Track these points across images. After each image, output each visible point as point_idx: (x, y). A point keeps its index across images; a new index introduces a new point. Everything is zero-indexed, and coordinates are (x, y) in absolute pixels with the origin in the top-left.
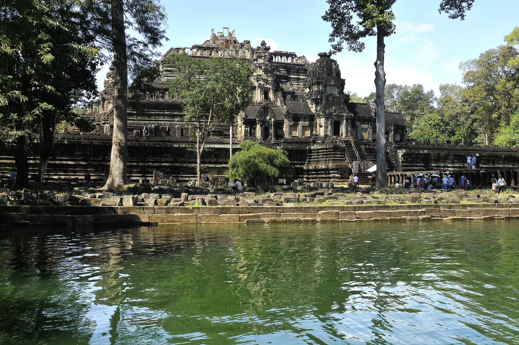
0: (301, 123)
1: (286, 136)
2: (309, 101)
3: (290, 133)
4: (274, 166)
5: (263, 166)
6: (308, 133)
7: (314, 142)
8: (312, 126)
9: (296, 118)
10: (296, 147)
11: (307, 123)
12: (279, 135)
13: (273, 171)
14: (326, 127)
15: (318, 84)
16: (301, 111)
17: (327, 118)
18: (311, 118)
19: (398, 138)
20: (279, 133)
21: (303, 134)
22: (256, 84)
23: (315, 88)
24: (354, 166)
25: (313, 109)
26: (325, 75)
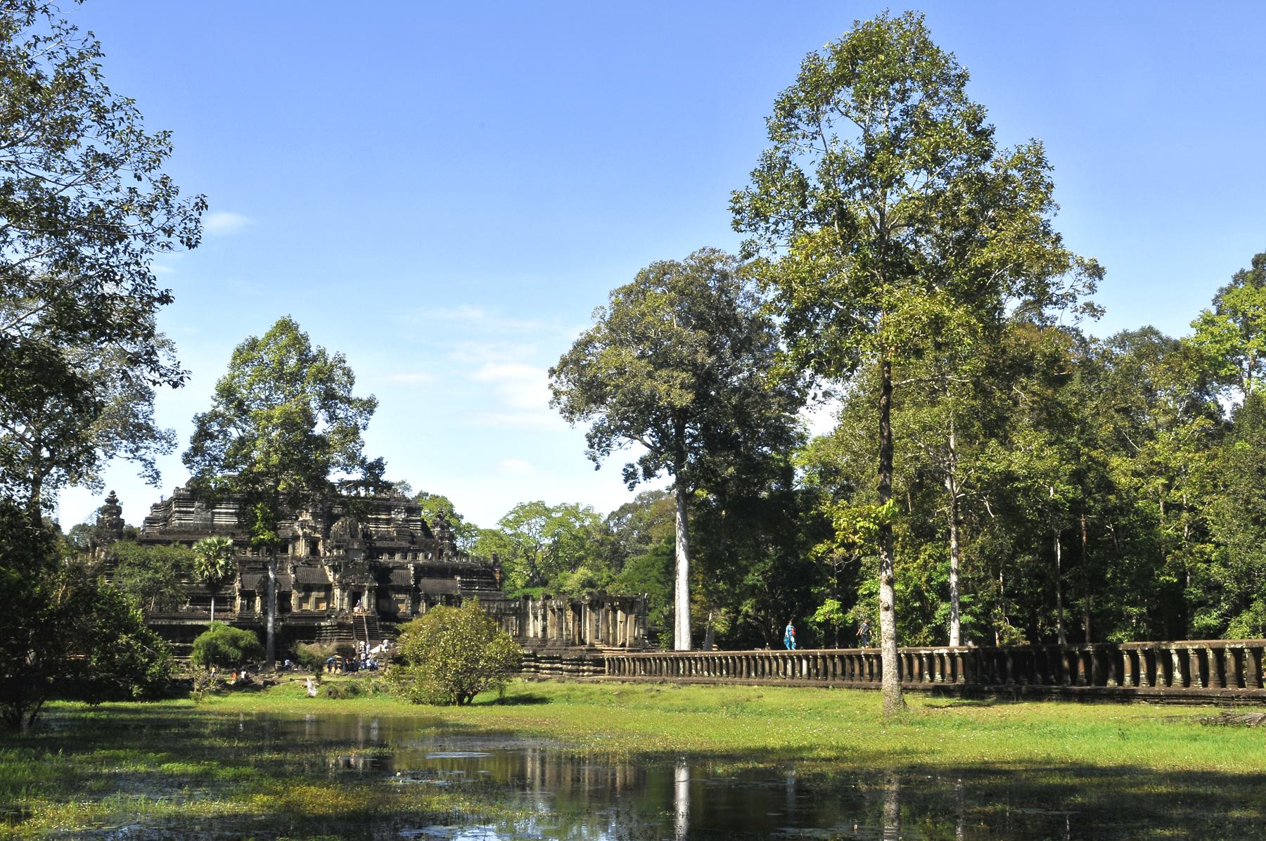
0: (314, 594)
1: (295, 610)
2: (327, 568)
3: (300, 606)
4: (237, 647)
5: (225, 648)
6: (323, 606)
7: (329, 617)
8: (328, 598)
9: (307, 589)
10: (303, 622)
11: (322, 594)
13: (235, 653)
14: (342, 600)
15: (338, 548)
16: (314, 580)
17: (343, 590)
18: (328, 588)
20: (286, 606)
21: (317, 606)
26: (347, 537)
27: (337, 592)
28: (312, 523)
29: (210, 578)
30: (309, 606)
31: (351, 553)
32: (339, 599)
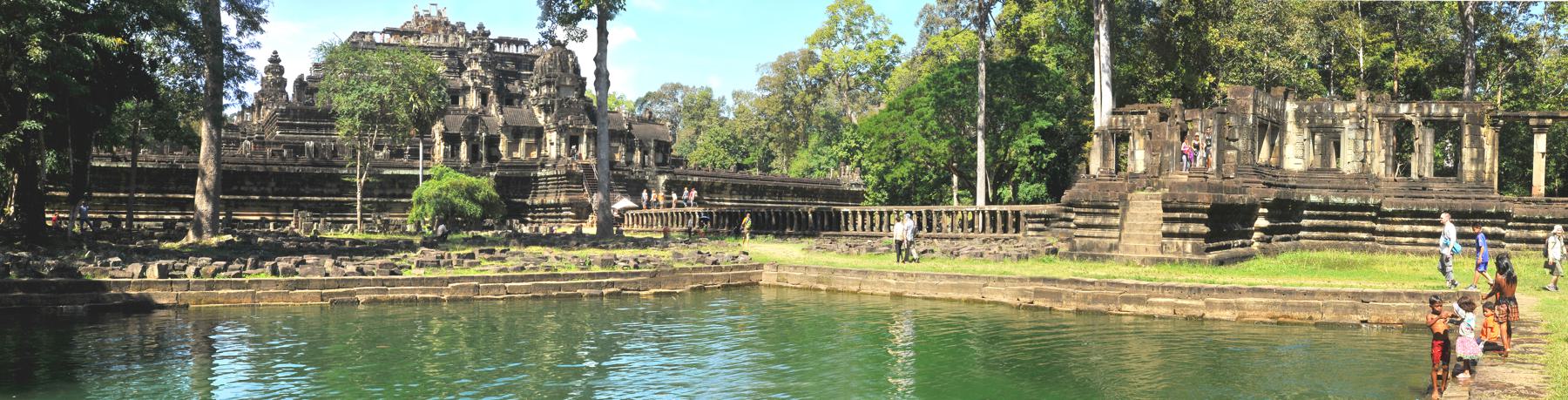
2: (536, 109)
3: (509, 154)
4: (475, 201)
5: (459, 201)
6: (534, 155)
7: (543, 166)
9: (516, 133)
10: (516, 172)
11: (532, 140)
12: (493, 157)
13: (474, 209)
15: (549, 84)
16: (525, 122)
19: (660, 160)
21: (528, 154)
22: (470, 83)
23: (544, 90)
24: (596, 200)
25: (541, 118)
26: (558, 72)
27: (552, 136)
28: (482, 73)
29: (419, 112)
30: (519, 154)
31: (562, 90)
32: (553, 145)
